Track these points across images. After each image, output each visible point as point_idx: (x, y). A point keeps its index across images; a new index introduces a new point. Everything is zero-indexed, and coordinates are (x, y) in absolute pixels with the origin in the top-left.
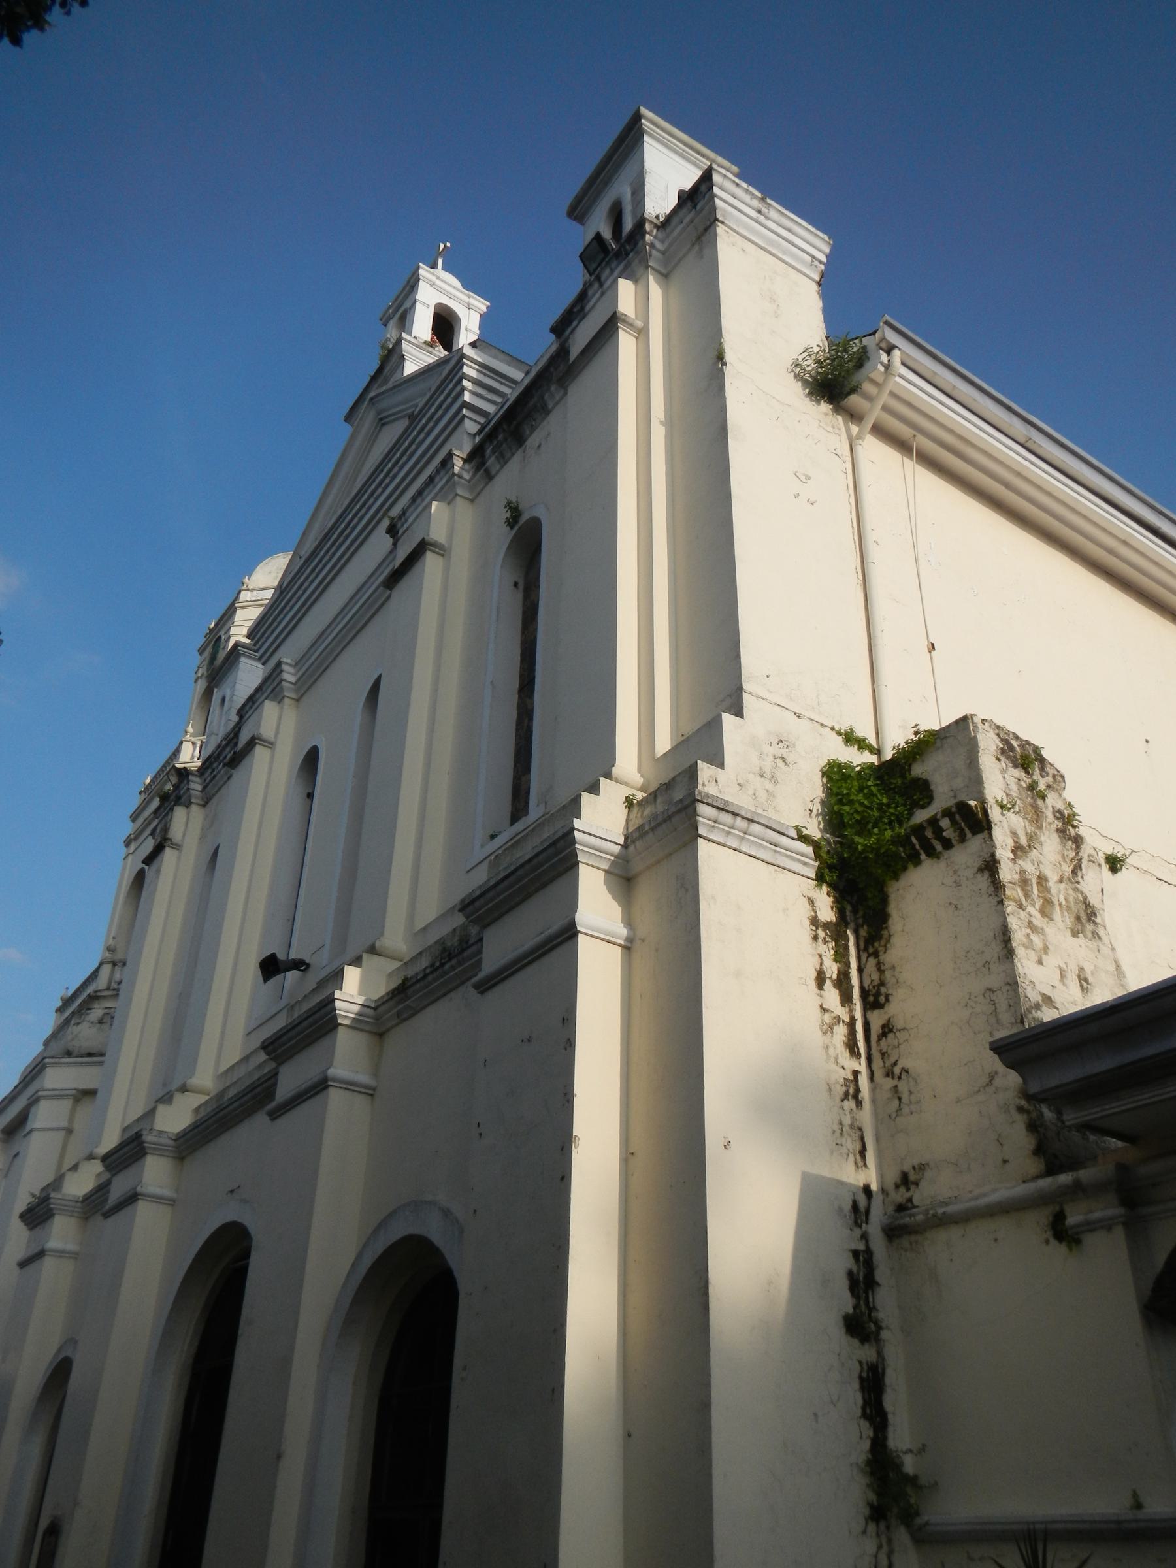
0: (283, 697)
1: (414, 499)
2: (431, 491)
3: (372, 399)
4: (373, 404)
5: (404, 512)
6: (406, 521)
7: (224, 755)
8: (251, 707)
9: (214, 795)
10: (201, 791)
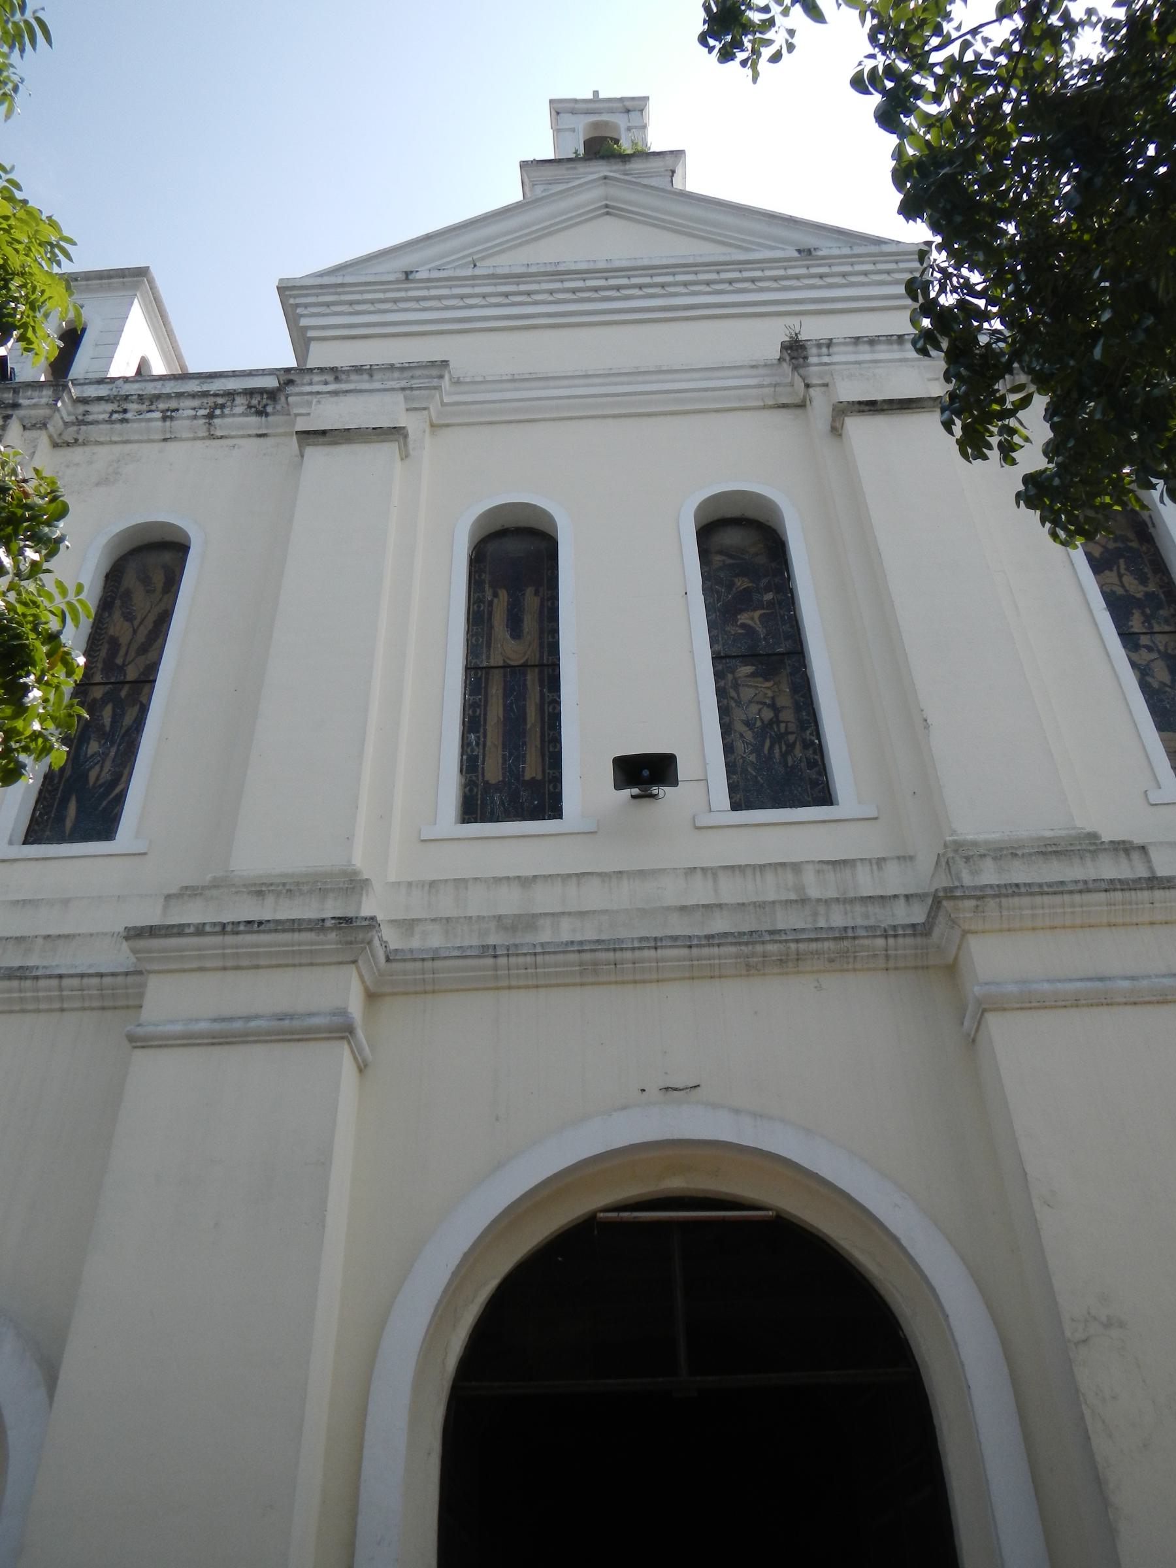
0: (425, 409)
1: (857, 340)
2: (893, 351)
4: (605, 183)
5: (830, 344)
6: (829, 355)
7: (173, 404)
8: (326, 383)
9: (98, 443)
10: (66, 424)
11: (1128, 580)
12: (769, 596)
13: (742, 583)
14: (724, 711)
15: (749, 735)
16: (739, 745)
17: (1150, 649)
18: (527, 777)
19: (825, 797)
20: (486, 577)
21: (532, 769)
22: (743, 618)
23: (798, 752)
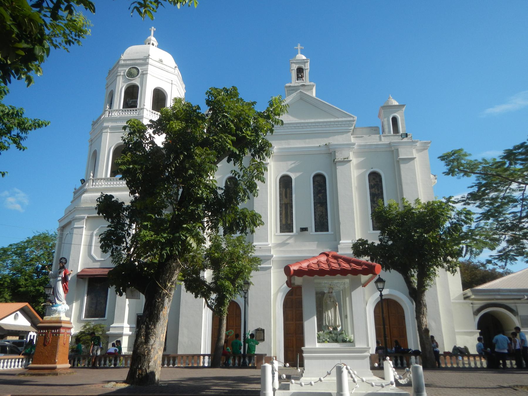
3: (300, 91)
11: (376, 190)
12: (323, 191)
13: (319, 188)
14: (315, 212)
15: (318, 217)
16: (317, 218)
17: (376, 204)
18: (288, 223)
19: (328, 231)
20: (281, 186)
21: (289, 222)
22: (319, 195)
23: (325, 220)
